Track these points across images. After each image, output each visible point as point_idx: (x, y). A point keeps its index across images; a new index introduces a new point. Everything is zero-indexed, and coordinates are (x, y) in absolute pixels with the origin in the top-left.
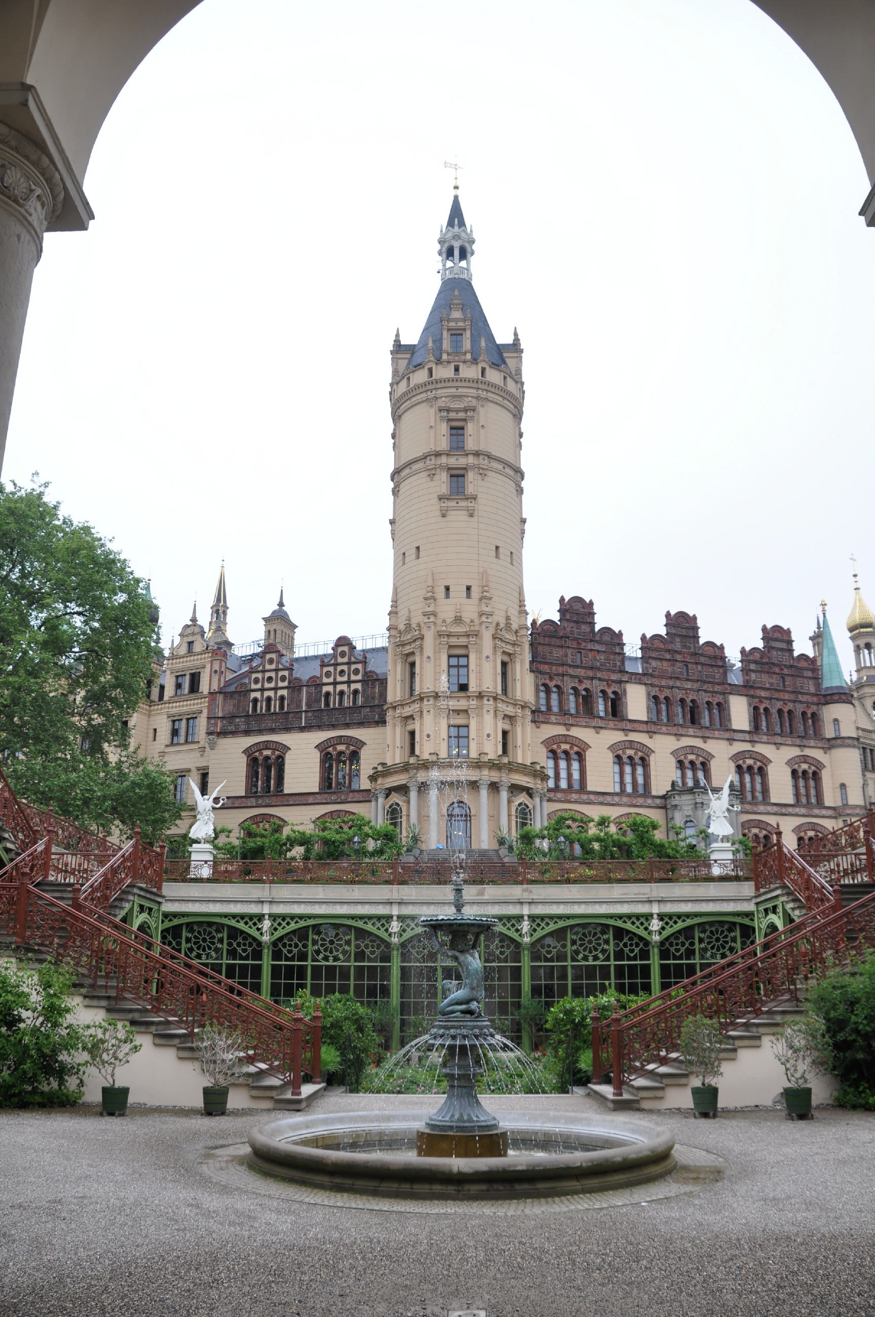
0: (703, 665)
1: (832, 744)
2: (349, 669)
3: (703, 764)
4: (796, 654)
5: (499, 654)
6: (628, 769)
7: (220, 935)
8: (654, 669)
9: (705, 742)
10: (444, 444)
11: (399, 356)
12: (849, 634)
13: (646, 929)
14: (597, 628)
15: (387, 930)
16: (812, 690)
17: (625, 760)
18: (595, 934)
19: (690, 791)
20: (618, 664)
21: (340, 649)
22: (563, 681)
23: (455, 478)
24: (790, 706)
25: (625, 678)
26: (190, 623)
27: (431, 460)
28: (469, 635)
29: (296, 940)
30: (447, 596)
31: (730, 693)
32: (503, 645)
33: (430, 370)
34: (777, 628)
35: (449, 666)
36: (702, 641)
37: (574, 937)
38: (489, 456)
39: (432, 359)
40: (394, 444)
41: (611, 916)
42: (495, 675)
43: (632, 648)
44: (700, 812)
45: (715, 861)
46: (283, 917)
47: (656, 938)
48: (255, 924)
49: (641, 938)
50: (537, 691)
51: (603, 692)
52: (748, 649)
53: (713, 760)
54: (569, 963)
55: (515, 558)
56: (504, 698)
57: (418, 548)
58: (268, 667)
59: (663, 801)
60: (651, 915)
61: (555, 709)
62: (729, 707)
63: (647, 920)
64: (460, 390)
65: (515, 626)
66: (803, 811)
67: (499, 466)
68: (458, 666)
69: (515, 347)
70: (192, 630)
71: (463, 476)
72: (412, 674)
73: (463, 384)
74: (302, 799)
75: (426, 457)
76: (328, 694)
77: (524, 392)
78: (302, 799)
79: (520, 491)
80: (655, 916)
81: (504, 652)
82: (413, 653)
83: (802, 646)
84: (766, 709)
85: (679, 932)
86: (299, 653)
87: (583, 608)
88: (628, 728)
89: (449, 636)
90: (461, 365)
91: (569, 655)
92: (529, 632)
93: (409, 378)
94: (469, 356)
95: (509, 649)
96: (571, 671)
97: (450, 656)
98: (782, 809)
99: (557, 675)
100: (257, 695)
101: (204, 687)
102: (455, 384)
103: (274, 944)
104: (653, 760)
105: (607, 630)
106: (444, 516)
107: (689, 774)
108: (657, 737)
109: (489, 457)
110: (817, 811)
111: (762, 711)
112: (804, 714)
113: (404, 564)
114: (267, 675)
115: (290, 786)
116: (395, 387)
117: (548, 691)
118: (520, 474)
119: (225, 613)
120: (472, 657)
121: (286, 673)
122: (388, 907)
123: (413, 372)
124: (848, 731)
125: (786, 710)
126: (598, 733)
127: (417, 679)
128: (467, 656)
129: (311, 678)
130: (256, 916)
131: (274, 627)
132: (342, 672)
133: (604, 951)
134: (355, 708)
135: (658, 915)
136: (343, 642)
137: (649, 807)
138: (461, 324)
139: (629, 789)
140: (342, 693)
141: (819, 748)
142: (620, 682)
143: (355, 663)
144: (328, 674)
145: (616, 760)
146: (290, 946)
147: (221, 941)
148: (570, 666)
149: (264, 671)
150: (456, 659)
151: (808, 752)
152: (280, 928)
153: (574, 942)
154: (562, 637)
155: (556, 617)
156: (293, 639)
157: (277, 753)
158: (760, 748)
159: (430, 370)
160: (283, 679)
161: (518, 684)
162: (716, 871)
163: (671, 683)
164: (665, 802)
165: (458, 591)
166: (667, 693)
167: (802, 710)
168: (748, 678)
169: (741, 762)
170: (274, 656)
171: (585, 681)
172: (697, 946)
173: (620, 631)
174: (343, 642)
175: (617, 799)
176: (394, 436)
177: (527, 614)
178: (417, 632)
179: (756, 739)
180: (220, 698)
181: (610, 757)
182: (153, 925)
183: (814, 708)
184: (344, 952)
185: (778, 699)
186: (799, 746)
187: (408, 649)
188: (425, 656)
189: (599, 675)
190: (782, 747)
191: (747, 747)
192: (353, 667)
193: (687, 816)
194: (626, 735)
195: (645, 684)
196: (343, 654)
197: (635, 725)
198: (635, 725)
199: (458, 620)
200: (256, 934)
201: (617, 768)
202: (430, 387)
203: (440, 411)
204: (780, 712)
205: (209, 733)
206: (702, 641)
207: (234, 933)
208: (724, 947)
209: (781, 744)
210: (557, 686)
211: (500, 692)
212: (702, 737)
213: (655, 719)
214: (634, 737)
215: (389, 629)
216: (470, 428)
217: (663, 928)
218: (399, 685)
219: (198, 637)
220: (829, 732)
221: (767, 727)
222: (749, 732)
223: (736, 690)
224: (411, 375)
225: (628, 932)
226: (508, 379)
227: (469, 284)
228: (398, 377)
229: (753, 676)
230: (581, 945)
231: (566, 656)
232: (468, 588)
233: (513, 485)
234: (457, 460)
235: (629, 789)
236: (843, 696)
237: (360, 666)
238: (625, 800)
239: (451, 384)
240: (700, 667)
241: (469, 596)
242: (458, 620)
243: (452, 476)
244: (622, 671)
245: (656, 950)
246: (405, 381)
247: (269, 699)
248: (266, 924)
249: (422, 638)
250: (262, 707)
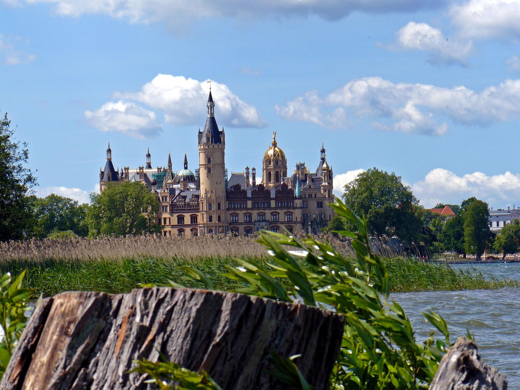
1: (294, 208)
61: (233, 207)
69: (222, 133)
78: (188, 226)
96: (235, 200)
101: (168, 200)
151: (289, 210)
158: (277, 211)
191: (274, 211)
197: (249, 209)
198: (249, 209)
214: (248, 211)
223: (273, 199)
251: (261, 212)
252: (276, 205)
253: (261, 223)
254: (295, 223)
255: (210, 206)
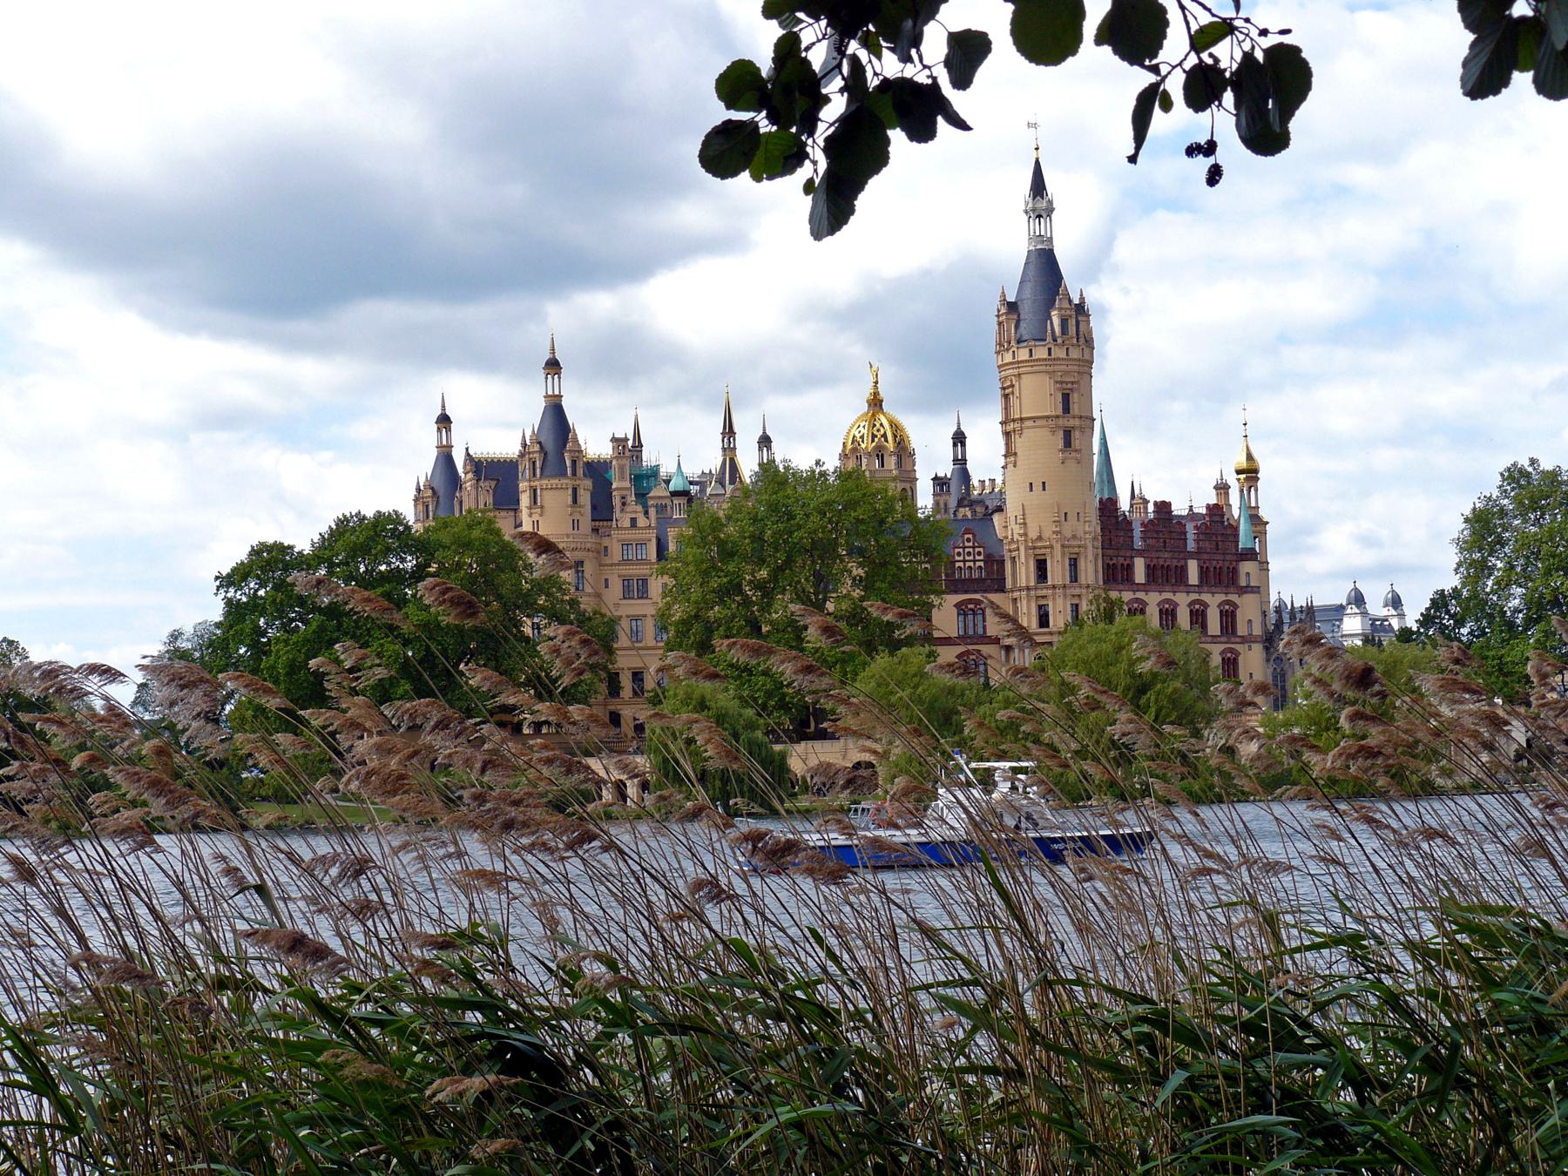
10: (1060, 411)
11: (1010, 316)
33: (1050, 349)
89: (1069, 547)
94: (1075, 341)
98: (1214, 640)
132: (969, 554)
134: (980, 580)
138: (1068, 312)
144: (959, 554)
159: (1050, 349)
198: (1137, 587)
220: (1243, 583)
227: (1052, 251)
251: (1167, 601)
254: (1245, 640)
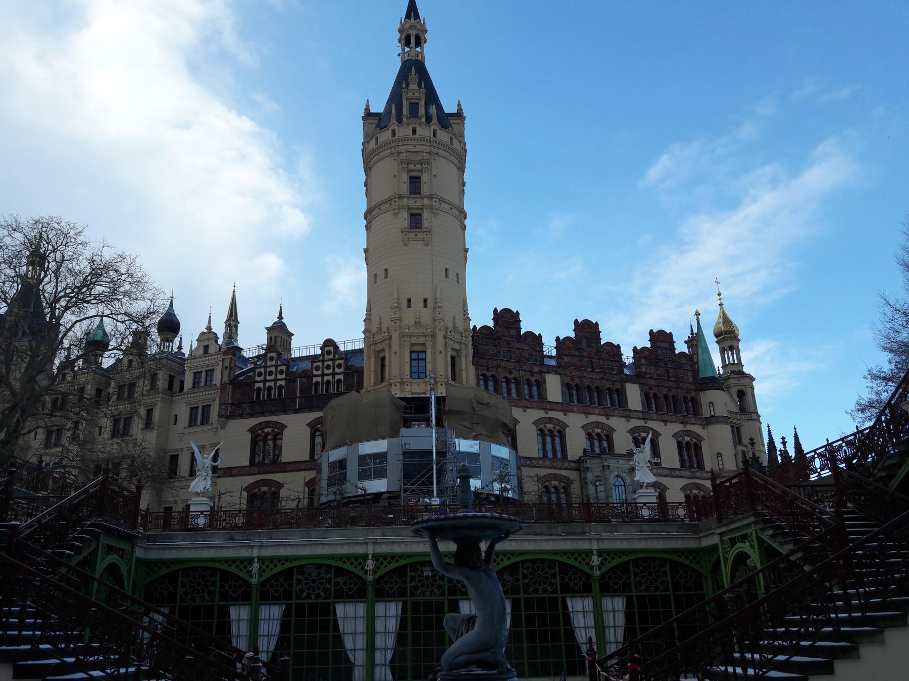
0: (604, 360)
2: (334, 364)
3: (607, 436)
4: (677, 352)
5: (449, 349)
6: (548, 439)
7: (213, 579)
8: (566, 363)
9: (608, 419)
10: (405, 188)
12: (716, 339)
13: (588, 564)
14: (522, 332)
15: (363, 568)
16: (691, 379)
17: (547, 432)
18: (543, 569)
19: (599, 456)
20: (539, 359)
21: (327, 349)
22: (497, 372)
23: (413, 217)
24: (674, 392)
25: (545, 369)
26: (205, 331)
27: (395, 202)
28: (426, 336)
29: (282, 580)
30: (409, 306)
31: (627, 382)
32: (452, 343)
34: (661, 332)
35: (411, 360)
36: (602, 343)
37: (526, 572)
38: (441, 200)
39: (395, 122)
40: (367, 190)
41: (556, 553)
42: (446, 365)
43: (549, 347)
44: (607, 473)
45: (644, 504)
46: (271, 559)
47: (597, 573)
48: (245, 567)
49: (584, 573)
50: (478, 379)
51: (528, 380)
52: (639, 348)
53: (615, 433)
54: (522, 596)
55: (460, 279)
56: (453, 383)
57: (386, 270)
58: (269, 363)
59: (577, 464)
60: (592, 551)
62: (626, 392)
63: (588, 556)
64: (417, 146)
65: (461, 329)
66: (688, 474)
67: (448, 207)
68: (418, 359)
69: (459, 115)
70: (208, 336)
71: (420, 215)
72: (383, 366)
73: (419, 142)
74: (295, 466)
75: (391, 199)
76: (317, 383)
77: (466, 151)
78: (295, 466)
79: (464, 228)
80: (595, 553)
81: (453, 349)
82: (383, 350)
83: (681, 347)
84: (655, 395)
85: (616, 567)
86: (295, 354)
87: (512, 317)
88: (548, 407)
90: (417, 127)
91: (501, 352)
92: (471, 335)
93: (377, 139)
94: (423, 120)
95: (457, 346)
96: (503, 364)
97: (411, 352)
99: (492, 367)
100: (261, 385)
101: (217, 379)
102: (412, 142)
103: (263, 584)
104: (568, 432)
105: (530, 334)
106: (406, 245)
107: (596, 443)
108: (570, 414)
109: (440, 200)
110: (698, 474)
111: (652, 395)
112: (685, 398)
113: (376, 282)
114: (269, 369)
115: (286, 457)
116: (366, 145)
117: (486, 380)
118: (463, 214)
119: (236, 327)
120: (429, 352)
121: (284, 368)
122: (364, 546)
123: (380, 133)
124: (721, 411)
125: (670, 395)
126: (524, 411)
127: (387, 368)
128: (425, 352)
129: (303, 372)
130: (246, 560)
131: (275, 334)
133: (552, 585)
135: (597, 551)
136: (329, 343)
137: (566, 469)
139: (550, 455)
140: (328, 382)
141: (699, 424)
142: (541, 372)
143: (338, 359)
144: (317, 368)
145: (539, 433)
146: (277, 586)
147: (214, 584)
148: (502, 360)
149: (266, 367)
150: (416, 354)
151: (689, 427)
152: (267, 570)
153: (525, 576)
154: (496, 339)
155: (491, 324)
156: (290, 344)
157: (276, 430)
158: (651, 424)
160: (281, 372)
161: (464, 373)
162: (645, 513)
163: (580, 374)
164: (579, 465)
165: (417, 303)
166: (577, 381)
167: (683, 395)
168: (639, 370)
169: (637, 435)
170: (274, 355)
171: (514, 372)
172: (632, 580)
173: (540, 334)
174: (329, 343)
175: (541, 462)
176: (366, 185)
177: (470, 320)
178: (386, 334)
179: (648, 417)
180: (230, 388)
181: (534, 430)
182: (123, 568)
183: (693, 394)
184: (325, 590)
185: (663, 386)
186: (682, 423)
187: (379, 347)
188: (393, 353)
189: (524, 368)
190: (669, 424)
191: (641, 423)
192: (337, 362)
193: (597, 476)
194: (547, 413)
195: (560, 374)
196: (329, 353)
197: (553, 406)
198: (553, 406)
199: (418, 324)
200: (245, 576)
201: (540, 439)
202: (394, 144)
203: (402, 163)
204: (666, 396)
205: (220, 416)
206: (602, 343)
207: (226, 575)
208: (656, 581)
209: (668, 421)
210: (493, 376)
211: (450, 379)
212: (606, 415)
213: (568, 401)
214: (552, 414)
215: (364, 332)
216: (425, 178)
217: (602, 564)
218: (372, 374)
219: (213, 341)
220: (706, 412)
221: (656, 408)
222: (642, 412)
224: (379, 135)
225: (572, 567)
226: (455, 141)
228: (368, 137)
229: (644, 369)
230: (531, 579)
231: (499, 352)
232: (425, 301)
233: (459, 223)
234: (415, 202)
235: (550, 455)
236: (714, 383)
237: (342, 362)
238: (547, 463)
239: (409, 142)
240: (602, 362)
241: (425, 306)
242: (418, 324)
243: (411, 215)
244: (542, 364)
245: (597, 583)
246: (373, 141)
247: (270, 388)
248: (256, 567)
249: (390, 338)
250: (264, 395)
252: (643, 404)
253: (612, 462)
255: (418, 357)
